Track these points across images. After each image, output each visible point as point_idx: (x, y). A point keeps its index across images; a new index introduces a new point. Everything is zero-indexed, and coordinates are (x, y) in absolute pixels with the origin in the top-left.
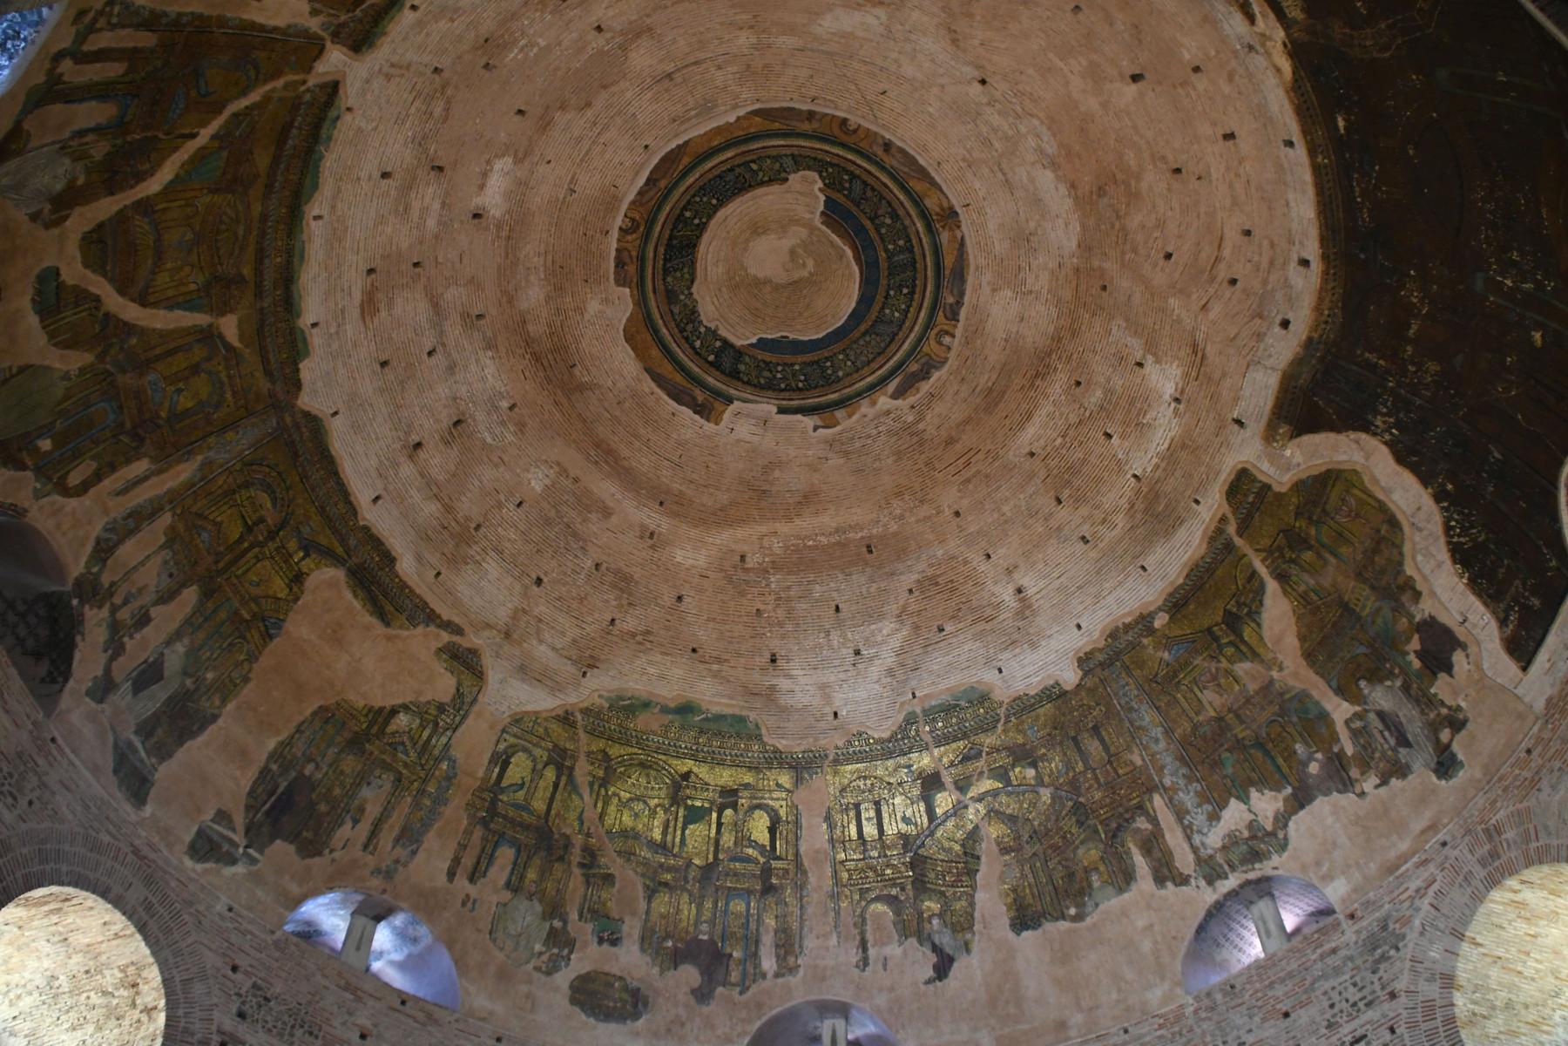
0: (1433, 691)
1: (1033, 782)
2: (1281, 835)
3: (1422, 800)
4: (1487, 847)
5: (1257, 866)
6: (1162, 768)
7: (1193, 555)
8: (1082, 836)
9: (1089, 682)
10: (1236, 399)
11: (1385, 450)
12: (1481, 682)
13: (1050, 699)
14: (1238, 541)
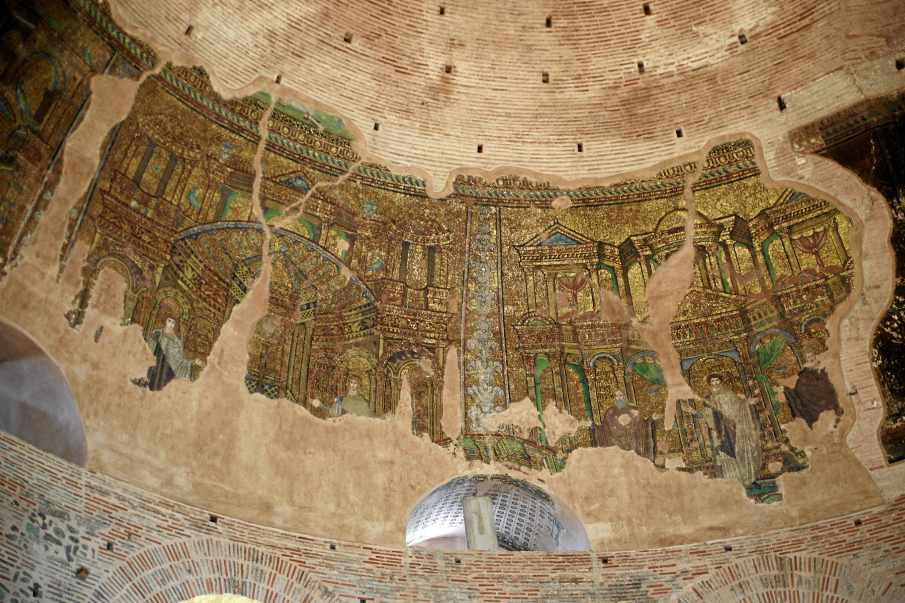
0: (783, 427)
1: (340, 254)
2: (560, 456)
3: (724, 504)
4: (776, 572)
5: (523, 468)
6: (473, 330)
7: (637, 172)
8: (360, 339)
9: (457, 206)
10: (799, 84)
11: (890, 223)
12: (838, 447)
13: (407, 191)
14: (688, 191)
